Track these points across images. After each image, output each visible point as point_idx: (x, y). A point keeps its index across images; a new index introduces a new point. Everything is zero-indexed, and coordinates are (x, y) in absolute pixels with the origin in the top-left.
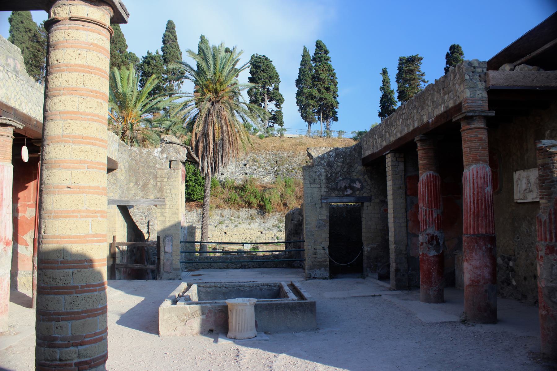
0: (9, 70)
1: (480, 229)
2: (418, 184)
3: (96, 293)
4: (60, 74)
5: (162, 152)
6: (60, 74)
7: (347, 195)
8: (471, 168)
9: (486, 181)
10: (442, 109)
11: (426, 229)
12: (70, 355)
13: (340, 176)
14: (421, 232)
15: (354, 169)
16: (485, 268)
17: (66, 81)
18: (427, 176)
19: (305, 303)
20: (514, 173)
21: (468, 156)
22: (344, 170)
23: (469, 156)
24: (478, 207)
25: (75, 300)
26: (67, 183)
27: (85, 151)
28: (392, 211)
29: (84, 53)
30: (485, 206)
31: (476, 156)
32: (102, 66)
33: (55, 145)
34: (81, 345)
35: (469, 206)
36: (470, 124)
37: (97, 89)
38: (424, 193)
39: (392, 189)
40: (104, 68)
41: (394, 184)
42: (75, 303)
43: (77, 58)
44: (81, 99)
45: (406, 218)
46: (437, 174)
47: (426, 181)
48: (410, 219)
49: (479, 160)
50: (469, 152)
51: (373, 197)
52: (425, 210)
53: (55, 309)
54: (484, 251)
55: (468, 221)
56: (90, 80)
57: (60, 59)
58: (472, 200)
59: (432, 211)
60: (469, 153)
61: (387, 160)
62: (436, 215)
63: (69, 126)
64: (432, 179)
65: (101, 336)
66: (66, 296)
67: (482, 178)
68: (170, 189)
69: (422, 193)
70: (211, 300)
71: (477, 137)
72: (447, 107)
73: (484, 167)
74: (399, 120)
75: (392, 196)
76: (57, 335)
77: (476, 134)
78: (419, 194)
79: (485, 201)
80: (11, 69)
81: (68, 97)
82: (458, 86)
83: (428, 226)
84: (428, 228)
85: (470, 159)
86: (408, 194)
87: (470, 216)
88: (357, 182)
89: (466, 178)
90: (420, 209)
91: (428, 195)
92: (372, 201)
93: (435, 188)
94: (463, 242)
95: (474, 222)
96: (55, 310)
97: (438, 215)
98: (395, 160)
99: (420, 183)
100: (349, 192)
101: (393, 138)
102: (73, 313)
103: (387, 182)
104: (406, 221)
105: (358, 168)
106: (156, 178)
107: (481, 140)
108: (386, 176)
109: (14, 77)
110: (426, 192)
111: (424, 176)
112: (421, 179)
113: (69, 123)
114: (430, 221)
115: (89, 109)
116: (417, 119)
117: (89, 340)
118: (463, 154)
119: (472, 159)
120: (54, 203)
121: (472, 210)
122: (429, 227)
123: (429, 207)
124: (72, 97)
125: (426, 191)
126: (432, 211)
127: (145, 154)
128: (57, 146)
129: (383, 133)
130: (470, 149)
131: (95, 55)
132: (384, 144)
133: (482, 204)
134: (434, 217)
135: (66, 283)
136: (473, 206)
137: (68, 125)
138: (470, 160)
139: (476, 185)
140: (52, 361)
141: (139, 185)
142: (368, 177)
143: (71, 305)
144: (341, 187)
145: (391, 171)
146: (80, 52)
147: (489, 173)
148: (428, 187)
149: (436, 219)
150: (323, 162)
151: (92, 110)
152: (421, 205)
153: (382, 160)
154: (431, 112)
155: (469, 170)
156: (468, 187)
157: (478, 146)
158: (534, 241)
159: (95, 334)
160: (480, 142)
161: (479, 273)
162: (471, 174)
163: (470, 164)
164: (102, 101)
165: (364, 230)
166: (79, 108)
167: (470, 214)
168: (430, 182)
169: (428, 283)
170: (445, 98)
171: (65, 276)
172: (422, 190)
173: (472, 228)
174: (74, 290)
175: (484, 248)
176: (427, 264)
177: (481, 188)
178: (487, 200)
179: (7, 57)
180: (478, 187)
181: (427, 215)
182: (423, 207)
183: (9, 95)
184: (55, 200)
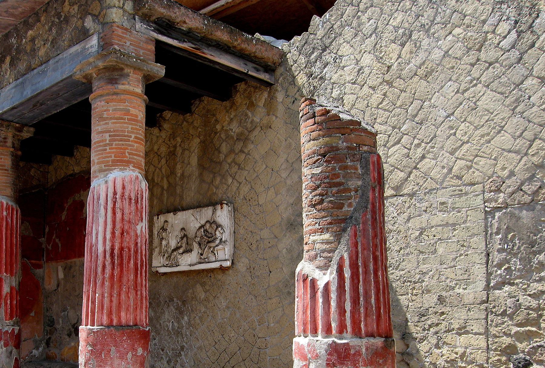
1: (123, 314)
8: (111, 176)
9: (139, 207)
20: (155, 218)
21: (106, 150)
23: (108, 150)
24: (121, 264)
30: (136, 264)
31: (125, 153)
35: (100, 262)
36: (116, 83)
49: (128, 163)
50: (108, 142)
54: (128, 363)
55: (97, 295)
58: (108, 248)
60: (108, 144)
67: (133, 201)
71: (127, 112)
73: (137, 178)
77: (127, 106)
79: (136, 252)
85: (111, 157)
87: (103, 283)
89: (99, 199)
93: (9, 232)
95: (111, 296)
97: (12, 288)
107: (133, 120)
119: (113, 158)
130: (110, 136)
138: (110, 159)
139: (119, 215)
147: (146, 195)
149: (9, 298)
155: (106, 182)
156: (101, 221)
158: (187, 343)
160: (132, 124)
163: (107, 168)
167: (104, 279)
175: (130, 355)
177: (129, 222)
178: (139, 251)
180: (123, 219)
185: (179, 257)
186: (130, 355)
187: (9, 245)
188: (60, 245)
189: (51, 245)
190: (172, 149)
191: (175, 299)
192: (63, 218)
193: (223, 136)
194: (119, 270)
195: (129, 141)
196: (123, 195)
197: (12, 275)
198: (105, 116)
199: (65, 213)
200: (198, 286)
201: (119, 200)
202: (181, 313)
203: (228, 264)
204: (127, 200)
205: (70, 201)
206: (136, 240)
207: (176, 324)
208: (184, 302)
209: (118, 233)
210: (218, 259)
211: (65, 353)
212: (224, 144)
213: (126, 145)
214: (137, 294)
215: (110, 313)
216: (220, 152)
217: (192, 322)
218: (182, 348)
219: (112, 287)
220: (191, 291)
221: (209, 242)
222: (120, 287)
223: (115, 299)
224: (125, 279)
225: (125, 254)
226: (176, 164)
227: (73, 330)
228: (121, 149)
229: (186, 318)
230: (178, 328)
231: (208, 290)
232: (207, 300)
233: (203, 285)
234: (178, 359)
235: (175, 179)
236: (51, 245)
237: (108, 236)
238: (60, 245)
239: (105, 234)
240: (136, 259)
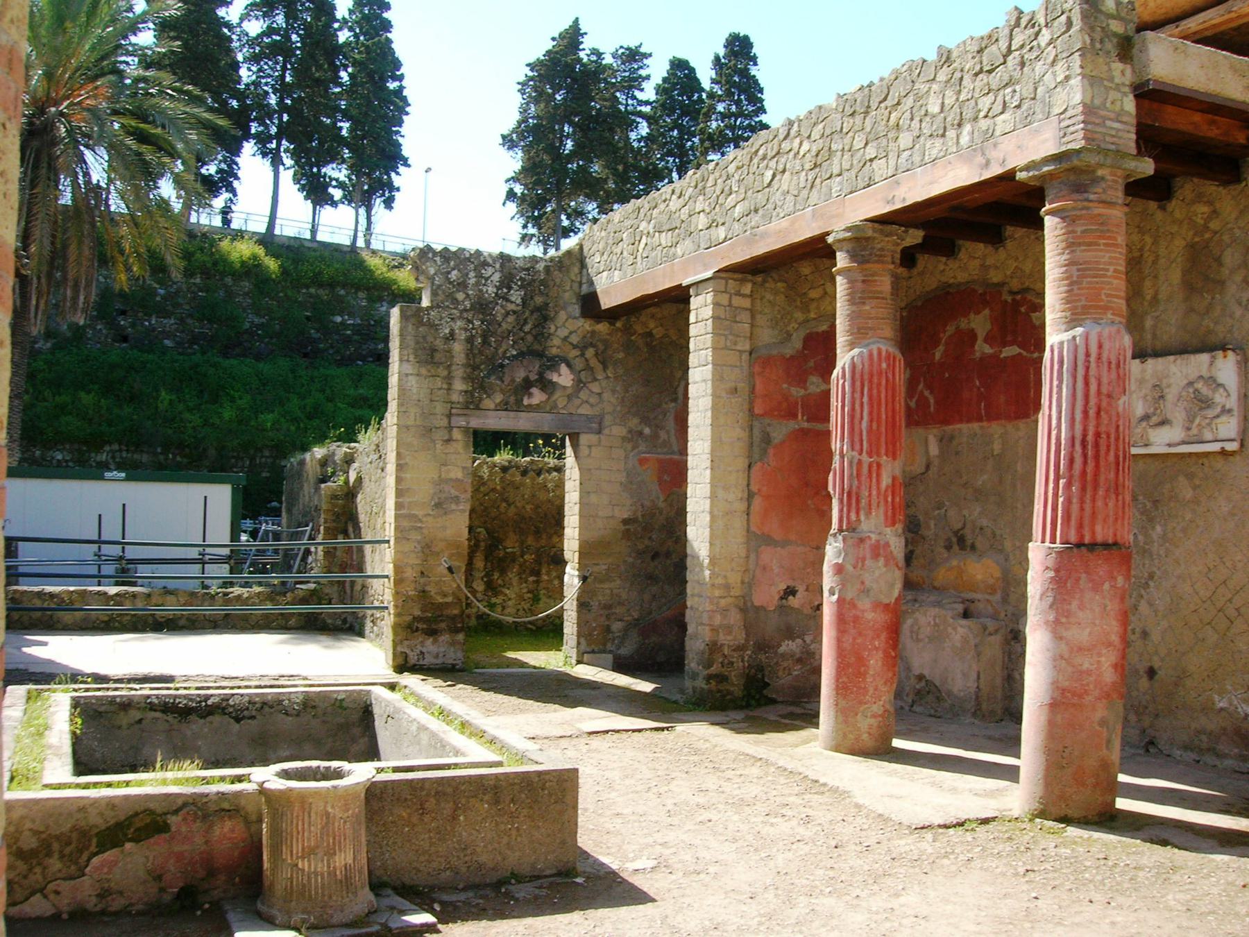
1: (1098, 528)
7: (530, 408)
11: (858, 520)
13: (513, 346)
15: (557, 328)
16: (1104, 651)
18: (871, 355)
22: (527, 328)
24: (1097, 457)
28: (708, 464)
30: (1117, 457)
38: (857, 407)
41: (718, 378)
45: (748, 485)
46: (899, 356)
48: (759, 490)
50: (1075, 279)
51: (608, 420)
52: (855, 461)
62: (890, 481)
64: (884, 365)
67: (1113, 366)
79: (1117, 439)
84: (862, 518)
85: (1079, 300)
86: (757, 411)
88: (564, 368)
91: (871, 413)
92: (606, 431)
93: (890, 393)
95: (1082, 501)
97: (894, 478)
98: (726, 302)
100: (537, 397)
103: (691, 372)
104: (746, 495)
114: (870, 495)
119: (1083, 303)
123: (870, 454)
125: (865, 399)
126: (879, 465)
133: (1108, 447)
138: (1079, 304)
142: (596, 355)
144: (513, 381)
148: (870, 390)
150: (460, 296)
157: (1105, 263)
158: (1159, 569)
161: (1086, 666)
168: (880, 373)
169: (851, 693)
175: (1106, 586)
176: (852, 631)
177: (1109, 396)
180: (1099, 392)
185: (1150, 431)
186: (1106, 586)
187: (890, 414)
188: (932, 401)
189: (914, 400)
190: (1137, 254)
191: (1141, 498)
192: (938, 356)
193: (1226, 238)
194: (1093, 464)
195: (1104, 276)
196: (1099, 358)
197: (894, 458)
199: (941, 348)
200: (1181, 478)
201: (1093, 365)
202: (1151, 520)
203: (1232, 447)
204: (1106, 364)
205: (950, 329)
206: (1118, 421)
207: (1140, 537)
208: (1155, 503)
209: (1092, 413)
210: (1219, 438)
211: (941, 577)
212: (1228, 252)
213: (1103, 283)
214: (1117, 501)
215: (1080, 526)
216: (1221, 265)
217: (1170, 535)
218: (1151, 576)
219: (1083, 489)
220: (1168, 486)
221: (1201, 409)
222: (1095, 488)
223: (1088, 507)
224: (1102, 478)
225: (1103, 442)
226: (1144, 279)
227: (954, 540)
228: (1096, 288)
229: (1159, 529)
230: (1145, 543)
231: (1199, 486)
232: (1196, 502)
233: (1190, 476)
234: (1143, 592)
235: (1142, 304)
236: (914, 400)
237: (1079, 416)
238: (932, 401)
240: (1117, 449)
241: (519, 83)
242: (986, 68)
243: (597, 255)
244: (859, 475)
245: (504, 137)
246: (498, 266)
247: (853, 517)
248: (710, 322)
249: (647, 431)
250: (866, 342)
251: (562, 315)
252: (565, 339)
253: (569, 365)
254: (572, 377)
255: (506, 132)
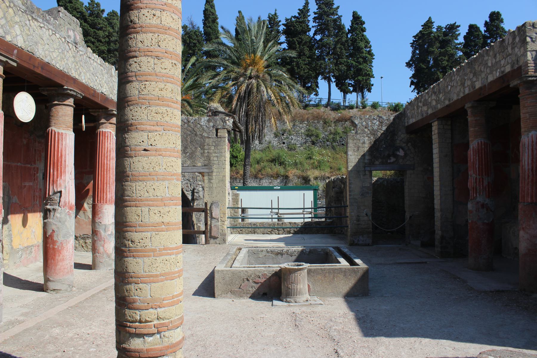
0: (70, 42)
2: (468, 152)
3: (173, 256)
4: (135, 35)
5: (209, 121)
6: (135, 35)
7: (390, 163)
8: (530, 134)
10: (498, 74)
12: (150, 316)
13: (384, 144)
14: (471, 200)
17: (142, 42)
19: (357, 268)
22: (388, 138)
25: (153, 263)
26: (145, 146)
27: (161, 112)
28: (439, 179)
29: (158, 13)
32: (175, 26)
33: (131, 107)
34: (160, 307)
35: (526, 174)
37: (172, 50)
38: (475, 160)
39: (438, 156)
40: (177, 29)
41: (440, 152)
42: (154, 266)
43: (151, 18)
44: (156, 60)
47: (477, 149)
50: (528, 118)
53: (134, 271)
55: (526, 189)
56: (165, 40)
57: (135, 20)
58: (530, 167)
59: (483, 179)
61: (433, 128)
62: (487, 183)
63: (145, 88)
64: (483, 147)
65: (178, 298)
66: (145, 258)
68: (217, 157)
69: (472, 161)
70: (262, 264)
72: (503, 72)
74: (447, 87)
75: (438, 164)
76: (137, 297)
78: (469, 161)
80: (72, 41)
81: (143, 59)
82: (518, 50)
83: (478, 194)
84: (478, 196)
87: (528, 184)
88: (401, 150)
89: (525, 145)
90: (469, 176)
94: (519, 210)
96: (134, 272)
97: (489, 183)
99: (471, 151)
100: (393, 160)
101: (440, 105)
102: (151, 276)
103: (433, 150)
105: (401, 136)
106: (202, 147)
108: (432, 144)
109: (74, 48)
110: (476, 159)
111: (474, 144)
112: (471, 147)
113: (145, 85)
115: (164, 70)
116: (468, 85)
117: (168, 303)
118: (521, 120)
120: (132, 165)
121: (530, 178)
122: (479, 194)
123: (479, 175)
124: (147, 58)
125: (477, 158)
126: (483, 179)
127: (192, 123)
128: (134, 108)
129: (430, 101)
130: (529, 115)
131: (169, 15)
132: (430, 112)
134: (484, 185)
135: (145, 245)
136: (531, 173)
137: (144, 86)
140: (132, 322)
141: (187, 153)
143: (150, 267)
145: (438, 139)
146: (154, 12)
151: (167, 71)
152: (471, 172)
153: (430, 126)
154: (484, 78)
155: (528, 137)
156: (526, 155)
159: (173, 297)
162: (530, 141)
164: (176, 62)
165: (407, 198)
166: (155, 69)
170: (501, 63)
171: (144, 239)
172: (472, 157)
173: (529, 196)
174: (152, 253)
179: (68, 29)
181: (478, 183)
182: (473, 176)
183: (70, 65)
184: (132, 163)
198: (526, 105)
237: (530, 162)
239: (528, 161)
241: (411, 43)
242: (503, 50)
243: (409, 114)
244: (476, 182)
245: (406, 63)
246: (378, 120)
247: (475, 195)
248: (437, 135)
249: (430, 168)
250: (477, 139)
251: (400, 133)
252: (401, 140)
253: (403, 149)
254: (404, 152)
255: (407, 62)
